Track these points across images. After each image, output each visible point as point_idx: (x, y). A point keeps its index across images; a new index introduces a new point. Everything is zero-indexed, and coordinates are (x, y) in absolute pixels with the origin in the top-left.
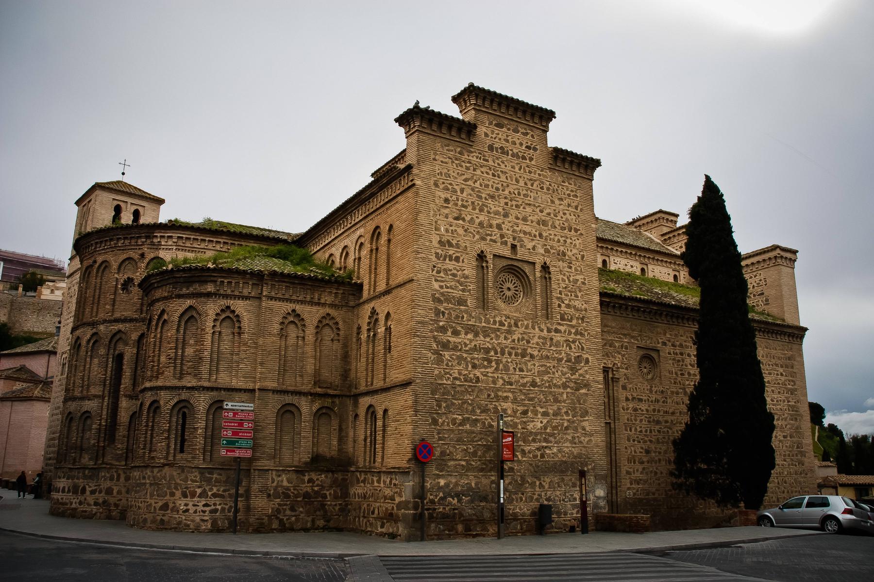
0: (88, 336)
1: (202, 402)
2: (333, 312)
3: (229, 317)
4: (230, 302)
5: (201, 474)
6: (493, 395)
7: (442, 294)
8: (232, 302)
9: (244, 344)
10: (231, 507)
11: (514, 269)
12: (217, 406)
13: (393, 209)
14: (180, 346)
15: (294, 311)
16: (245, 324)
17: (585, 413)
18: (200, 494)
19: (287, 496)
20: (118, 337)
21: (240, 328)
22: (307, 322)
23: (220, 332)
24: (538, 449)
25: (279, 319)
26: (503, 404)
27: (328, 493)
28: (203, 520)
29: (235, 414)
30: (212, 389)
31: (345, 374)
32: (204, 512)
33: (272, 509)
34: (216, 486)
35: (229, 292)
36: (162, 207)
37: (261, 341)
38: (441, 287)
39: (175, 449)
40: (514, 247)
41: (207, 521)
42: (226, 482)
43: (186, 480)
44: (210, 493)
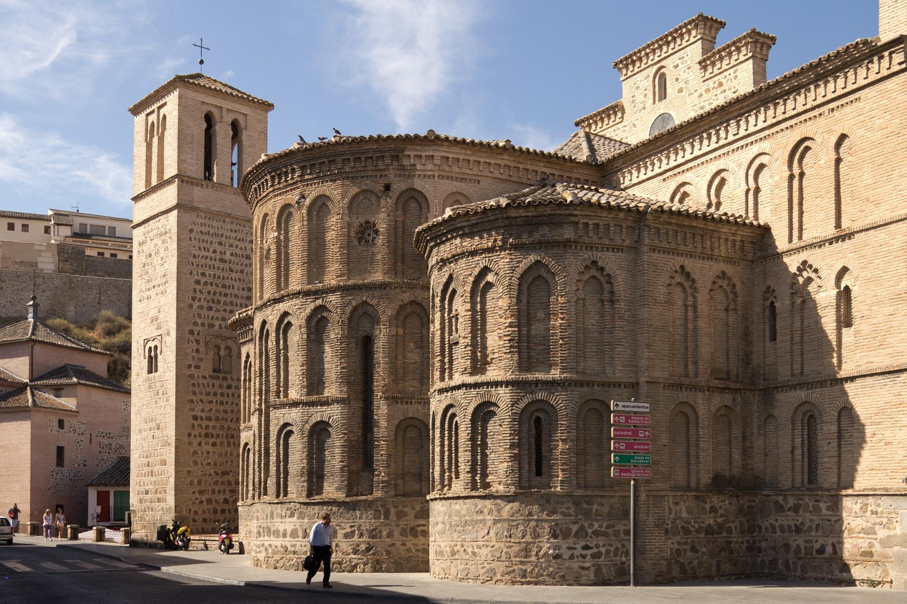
0: (308, 311)
2: (729, 270)
5: (577, 504)
8: (599, 254)
9: (620, 318)
10: (617, 549)
14: (524, 321)
15: (682, 267)
18: (577, 532)
19: (687, 531)
20: (361, 311)
21: (612, 292)
22: (699, 285)
23: (584, 299)
25: (664, 279)
27: (733, 526)
28: (583, 568)
29: (627, 418)
30: (581, 384)
31: (746, 359)
32: (584, 557)
33: (671, 549)
34: (597, 521)
35: (595, 239)
39: (529, 470)
41: (588, 569)
42: (610, 515)
44: (590, 531)
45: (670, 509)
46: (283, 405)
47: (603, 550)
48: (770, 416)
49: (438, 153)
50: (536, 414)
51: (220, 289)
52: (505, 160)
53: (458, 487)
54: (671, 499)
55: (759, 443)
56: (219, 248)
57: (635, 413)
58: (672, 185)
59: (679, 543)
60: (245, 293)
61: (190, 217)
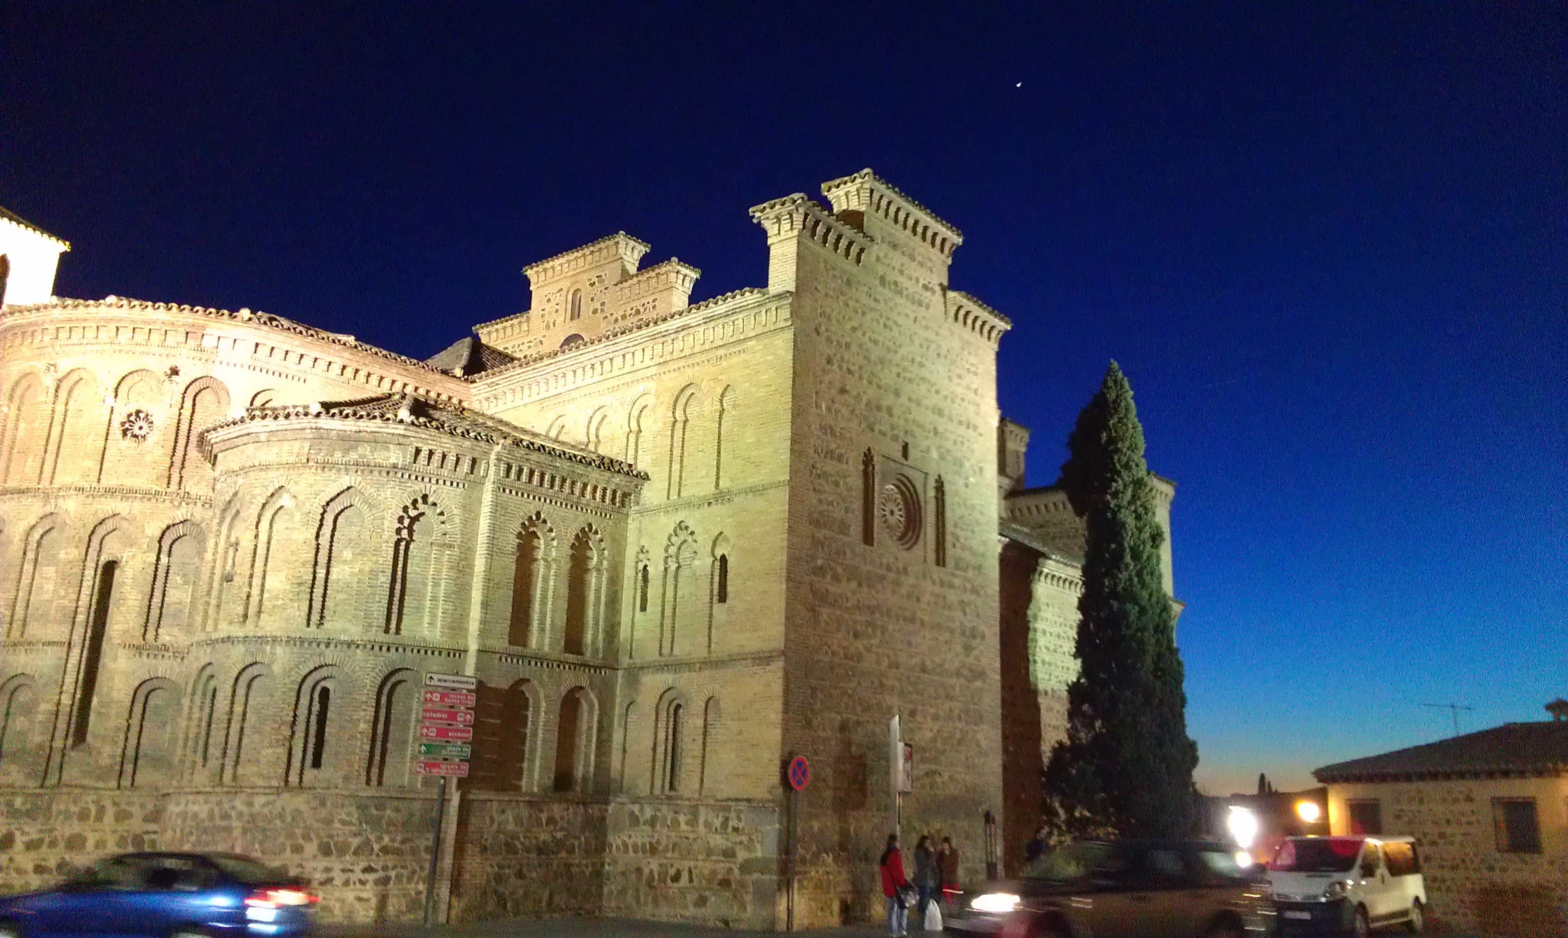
6: (876, 682)
7: (821, 513)
10: (414, 872)
13: (735, 360)
19: (510, 848)
20: (109, 525)
24: (927, 774)
26: (888, 697)
27: (576, 843)
28: (360, 899)
29: (443, 696)
34: (388, 832)
38: (820, 501)
40: (905, 447)
41: (368, 900)
43: (328, 822)
44: (376, 847)
45: (492, 820)
47: (393, 874)
50: (323, 684)
54: (495, 805)
55: (617, 736)
57: (453, 689)
59: (500, 867)
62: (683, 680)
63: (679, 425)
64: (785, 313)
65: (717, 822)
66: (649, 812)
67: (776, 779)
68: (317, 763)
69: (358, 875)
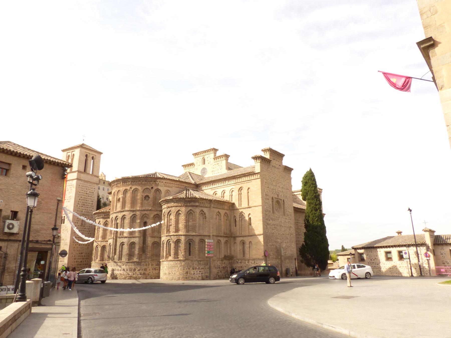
0: (131, 215)
1: (197, 240)
3: (203, 213)
4: (203, 209)
11: (278, 202)
12: (202, 241)
16: (207, 215)
17: (292, 242)
19: (219, 268)
25: (215, 214)
30: (199, 236)
31: (230, 231)
36: (102, 155)
37: (211, 221)
43: (193, 264)
46: (122, 237)
48: (235, 243)
49: (164, 181)
51: (85, 201)
52: (178, 183)
53: (170, 258)
55: (233, 248)
56: (86, 190)
58: (213, 191)
60: (92, 203)
61: (80, 182)
62: (244, 239)
63: (240, 194)
64: (259, 176)
65: (253, 262)
66: (240, 261)
67: (263, 255)
68: (190, 255)
69: (198, 273)
